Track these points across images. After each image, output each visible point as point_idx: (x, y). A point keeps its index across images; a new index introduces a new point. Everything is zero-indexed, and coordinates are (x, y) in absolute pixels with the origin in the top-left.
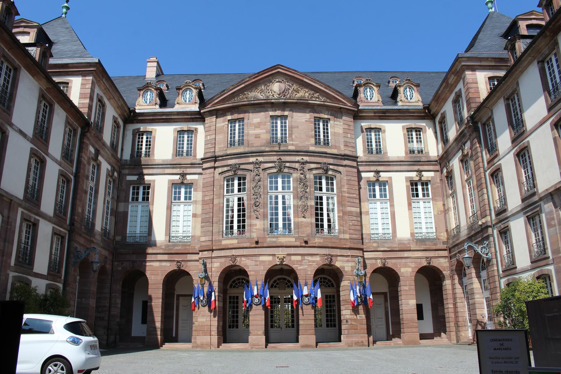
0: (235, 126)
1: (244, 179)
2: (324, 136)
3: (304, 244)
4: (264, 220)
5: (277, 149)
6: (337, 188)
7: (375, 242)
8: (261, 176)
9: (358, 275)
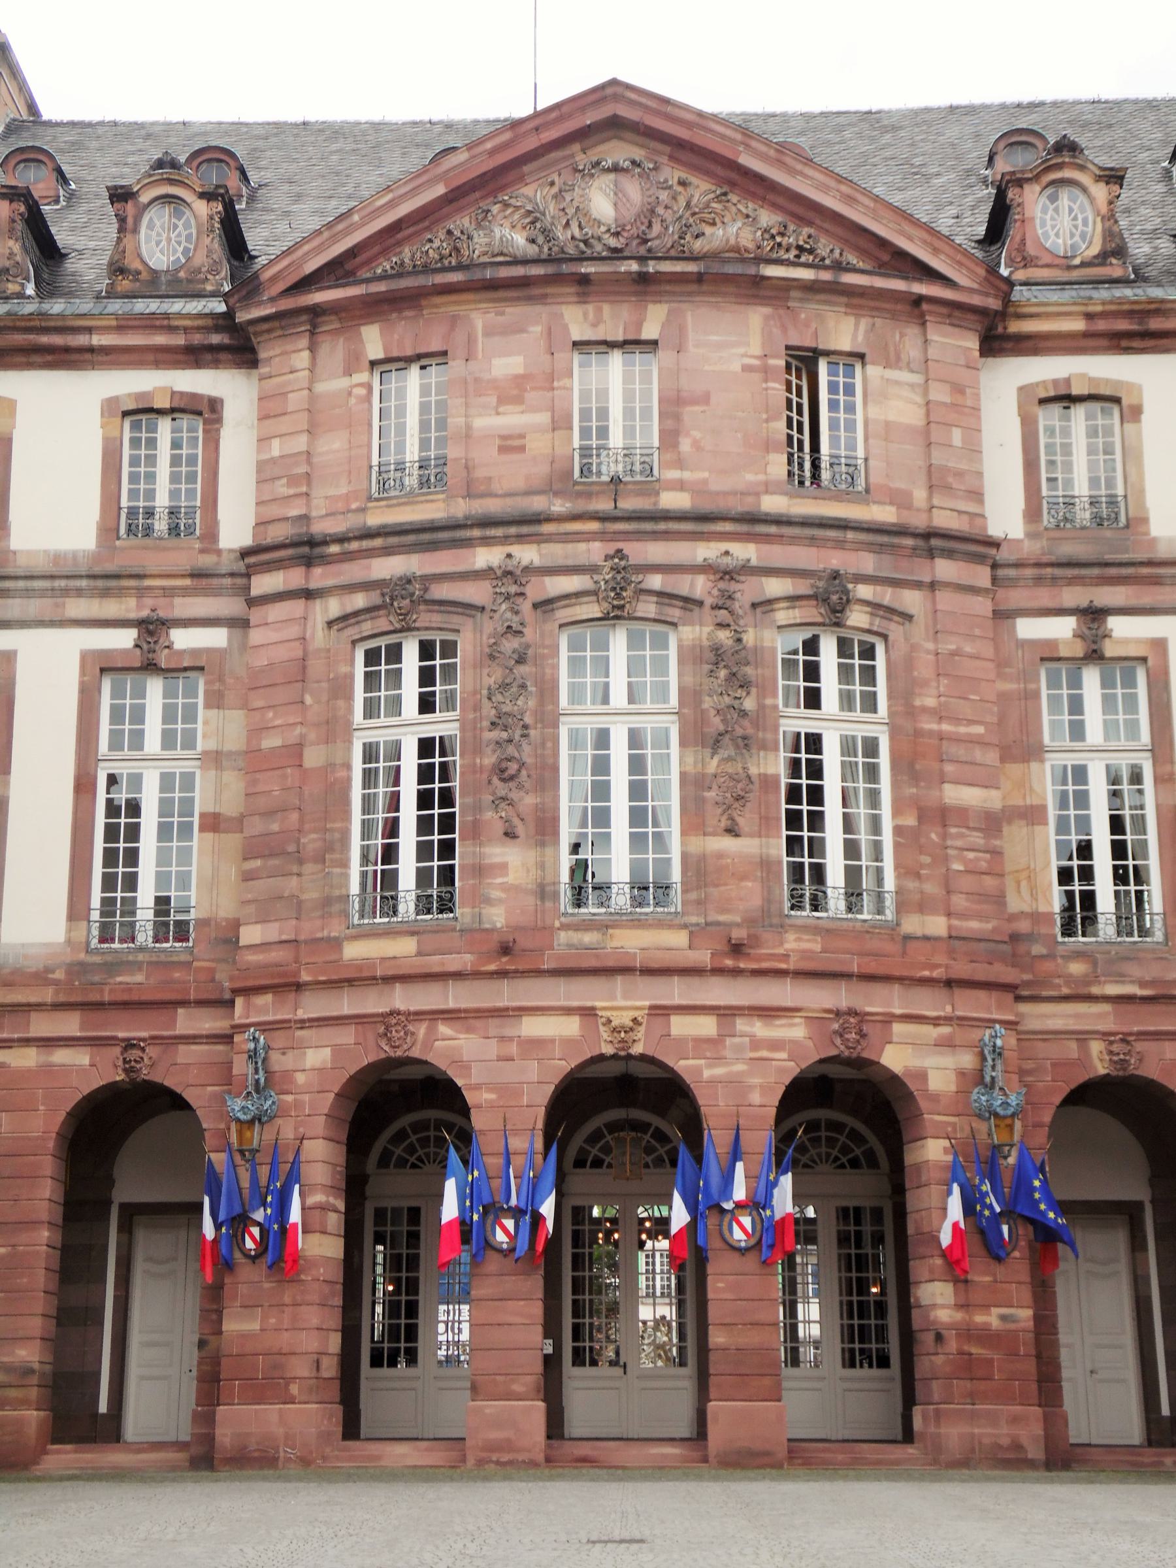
1: (449, 649)
5: (603, 505)
6: (890, 697)
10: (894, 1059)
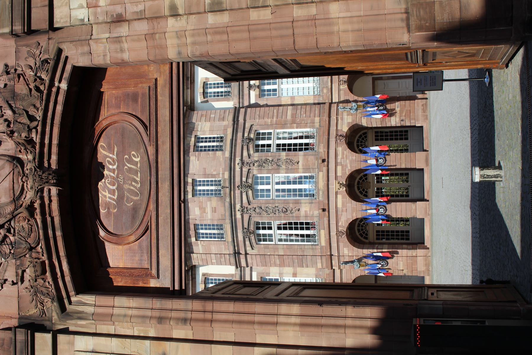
0: (203, 234)
1: (258, 223)
2: (214, 141)
3: (326, 163)
4: (301, 203)
5: (228, 190)
6: (268, 129)
7: (322, 90)
8: (255, 206)
9: (357, 110)
10: (345, 129)
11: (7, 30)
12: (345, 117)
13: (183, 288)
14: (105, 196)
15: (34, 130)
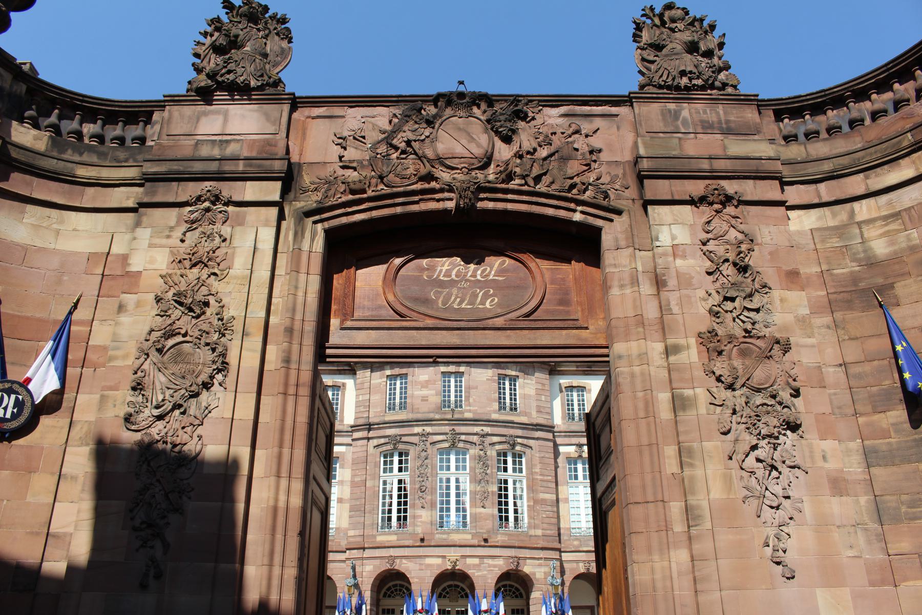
0: (395, 384)
1: (407, 454)
2: (511, 399)
3: (483, 543)
5: (449, 416)
6: (527, 468)
7: (577, 539)
8: (429, 451)
9: (552, 585)
10: (527, 569)
11: (642, 152)
12: (543, 569)
13: (328, 360)
14: (443, 266)
15: (523, 182)
